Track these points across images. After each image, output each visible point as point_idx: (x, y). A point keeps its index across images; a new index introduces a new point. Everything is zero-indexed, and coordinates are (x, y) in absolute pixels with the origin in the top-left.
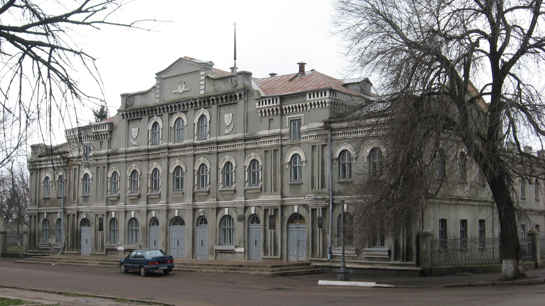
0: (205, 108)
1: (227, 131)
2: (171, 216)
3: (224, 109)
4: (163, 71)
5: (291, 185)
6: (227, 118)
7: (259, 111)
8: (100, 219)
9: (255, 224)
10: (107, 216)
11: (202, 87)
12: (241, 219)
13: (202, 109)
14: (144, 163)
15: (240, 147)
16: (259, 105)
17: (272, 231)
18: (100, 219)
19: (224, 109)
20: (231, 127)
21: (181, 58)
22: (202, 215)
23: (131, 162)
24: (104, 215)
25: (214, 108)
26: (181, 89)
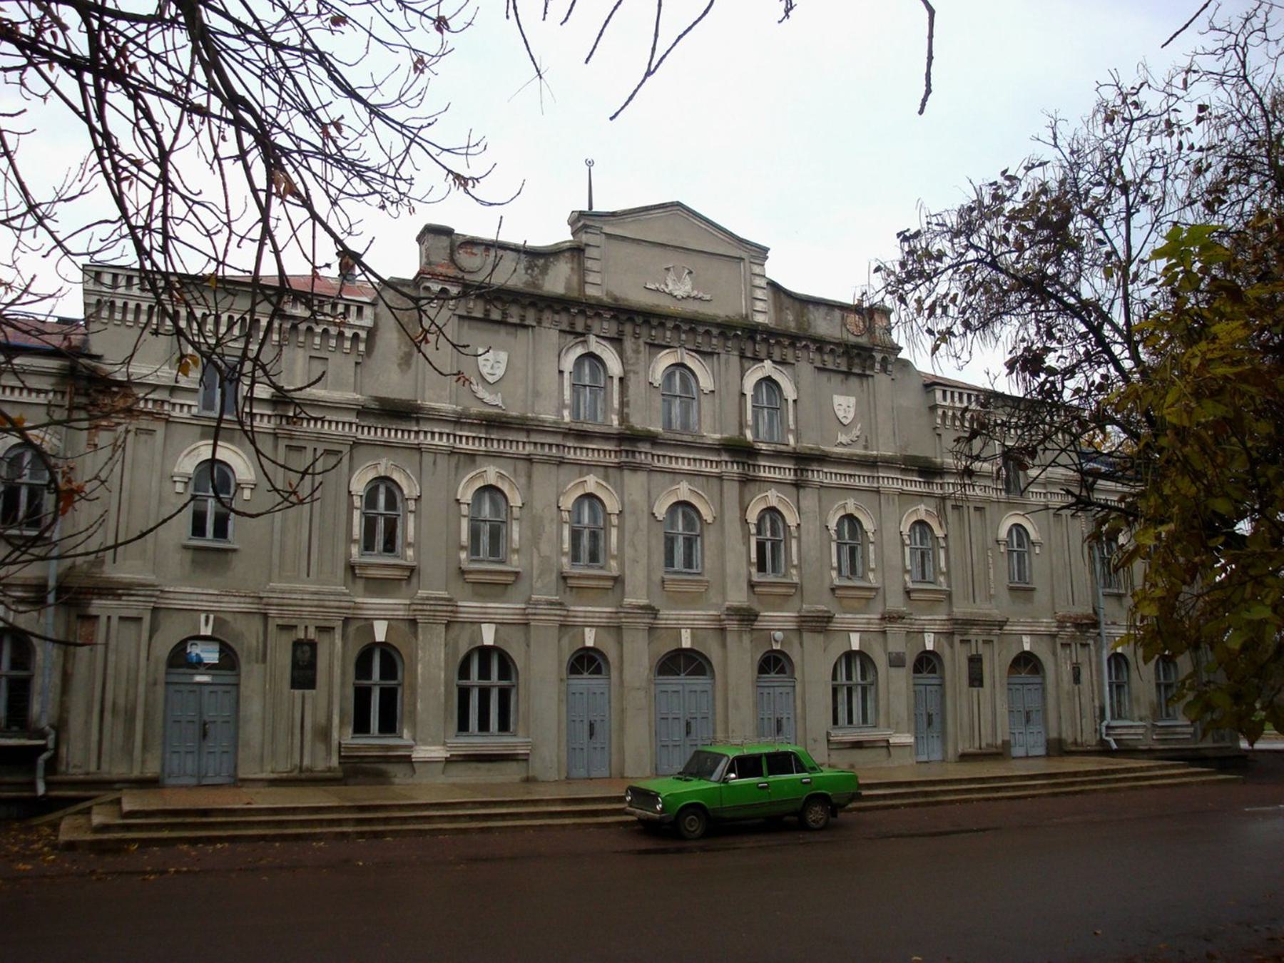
0: (774, 362)
1: (843, 438)
2: (667, 647)
3: (829, 380)
4: (613, 214)
5: (1011, 589)
6: (845, 405)
7: (940, 412)
8: (297, 644)
9: (682, 675)
10: (344, 637)
11: (760, 306)
12: (896, 661)
13: (768, 363)
14: (539, 471)
15: (891, 482)
16: (945, 398)
17: (975, 690)
18: (297, 644)
19: (829, 380)
20: (856, 432)
21: (679, 204)
22: (777, 647)
23: (472, 457)
24: (329, 630)
25: (805, 369)
26: (683, 288)
